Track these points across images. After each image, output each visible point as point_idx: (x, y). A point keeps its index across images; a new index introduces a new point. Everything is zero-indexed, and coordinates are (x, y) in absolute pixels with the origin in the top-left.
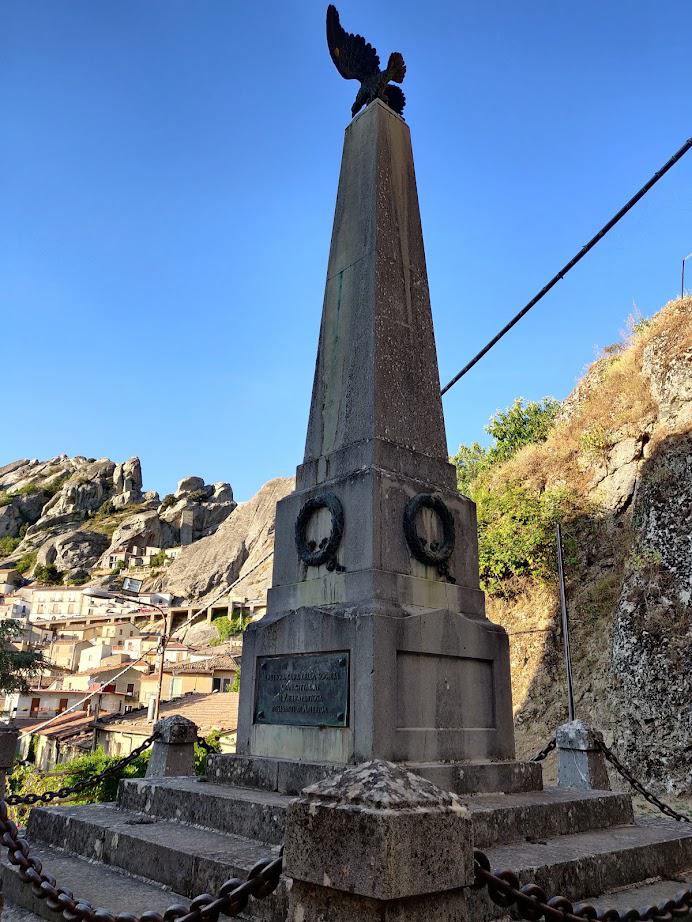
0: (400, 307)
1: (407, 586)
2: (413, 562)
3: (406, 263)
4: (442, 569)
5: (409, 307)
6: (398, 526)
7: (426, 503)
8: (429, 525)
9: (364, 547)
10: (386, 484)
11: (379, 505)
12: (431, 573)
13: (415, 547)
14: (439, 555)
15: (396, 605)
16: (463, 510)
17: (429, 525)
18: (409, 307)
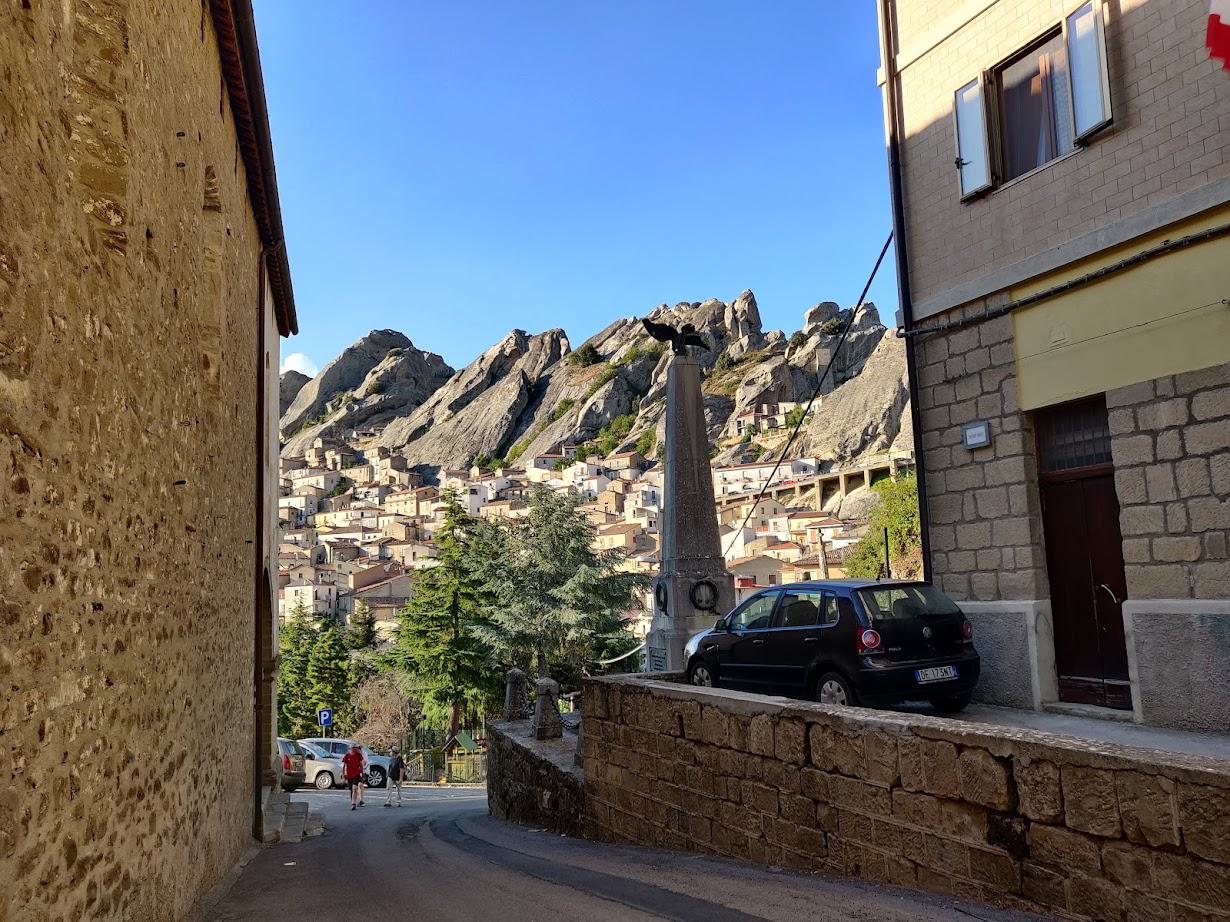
0: (690, 485)
1: (692, 622)
2: (696, 610)
3: (695, 457)
4: (712, 610)
5: (697, 482)
6: (687, 597)
7: (702, 583)
8: (704, 593)
9: (671, 607)
10: (679, 581)
11: (675, 591)
12: (706, 613)
13: (695, 603)
14: (709, 605)
15: (685, 630)
16: (725, 581)
17: (704, 593)
18: (697, 482)
